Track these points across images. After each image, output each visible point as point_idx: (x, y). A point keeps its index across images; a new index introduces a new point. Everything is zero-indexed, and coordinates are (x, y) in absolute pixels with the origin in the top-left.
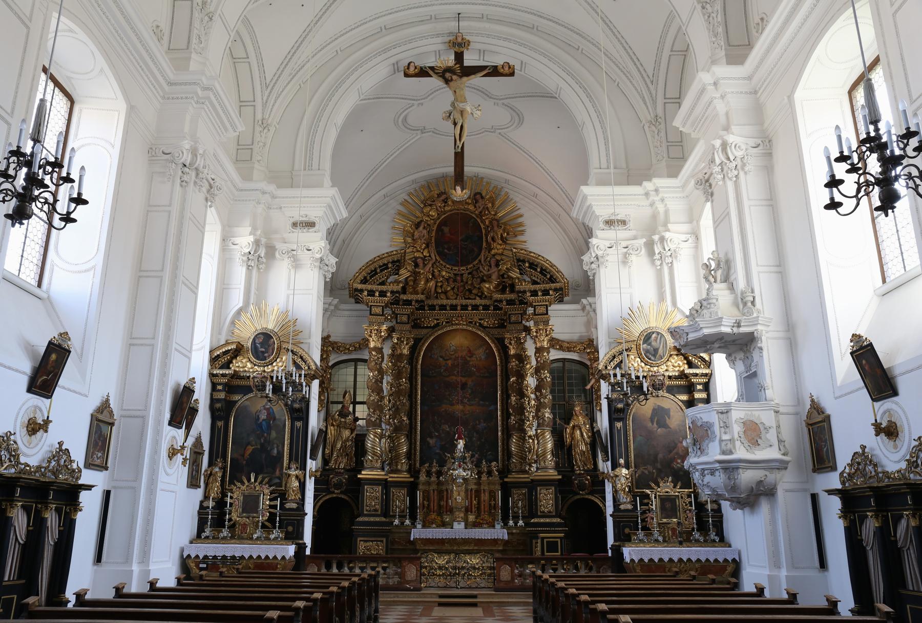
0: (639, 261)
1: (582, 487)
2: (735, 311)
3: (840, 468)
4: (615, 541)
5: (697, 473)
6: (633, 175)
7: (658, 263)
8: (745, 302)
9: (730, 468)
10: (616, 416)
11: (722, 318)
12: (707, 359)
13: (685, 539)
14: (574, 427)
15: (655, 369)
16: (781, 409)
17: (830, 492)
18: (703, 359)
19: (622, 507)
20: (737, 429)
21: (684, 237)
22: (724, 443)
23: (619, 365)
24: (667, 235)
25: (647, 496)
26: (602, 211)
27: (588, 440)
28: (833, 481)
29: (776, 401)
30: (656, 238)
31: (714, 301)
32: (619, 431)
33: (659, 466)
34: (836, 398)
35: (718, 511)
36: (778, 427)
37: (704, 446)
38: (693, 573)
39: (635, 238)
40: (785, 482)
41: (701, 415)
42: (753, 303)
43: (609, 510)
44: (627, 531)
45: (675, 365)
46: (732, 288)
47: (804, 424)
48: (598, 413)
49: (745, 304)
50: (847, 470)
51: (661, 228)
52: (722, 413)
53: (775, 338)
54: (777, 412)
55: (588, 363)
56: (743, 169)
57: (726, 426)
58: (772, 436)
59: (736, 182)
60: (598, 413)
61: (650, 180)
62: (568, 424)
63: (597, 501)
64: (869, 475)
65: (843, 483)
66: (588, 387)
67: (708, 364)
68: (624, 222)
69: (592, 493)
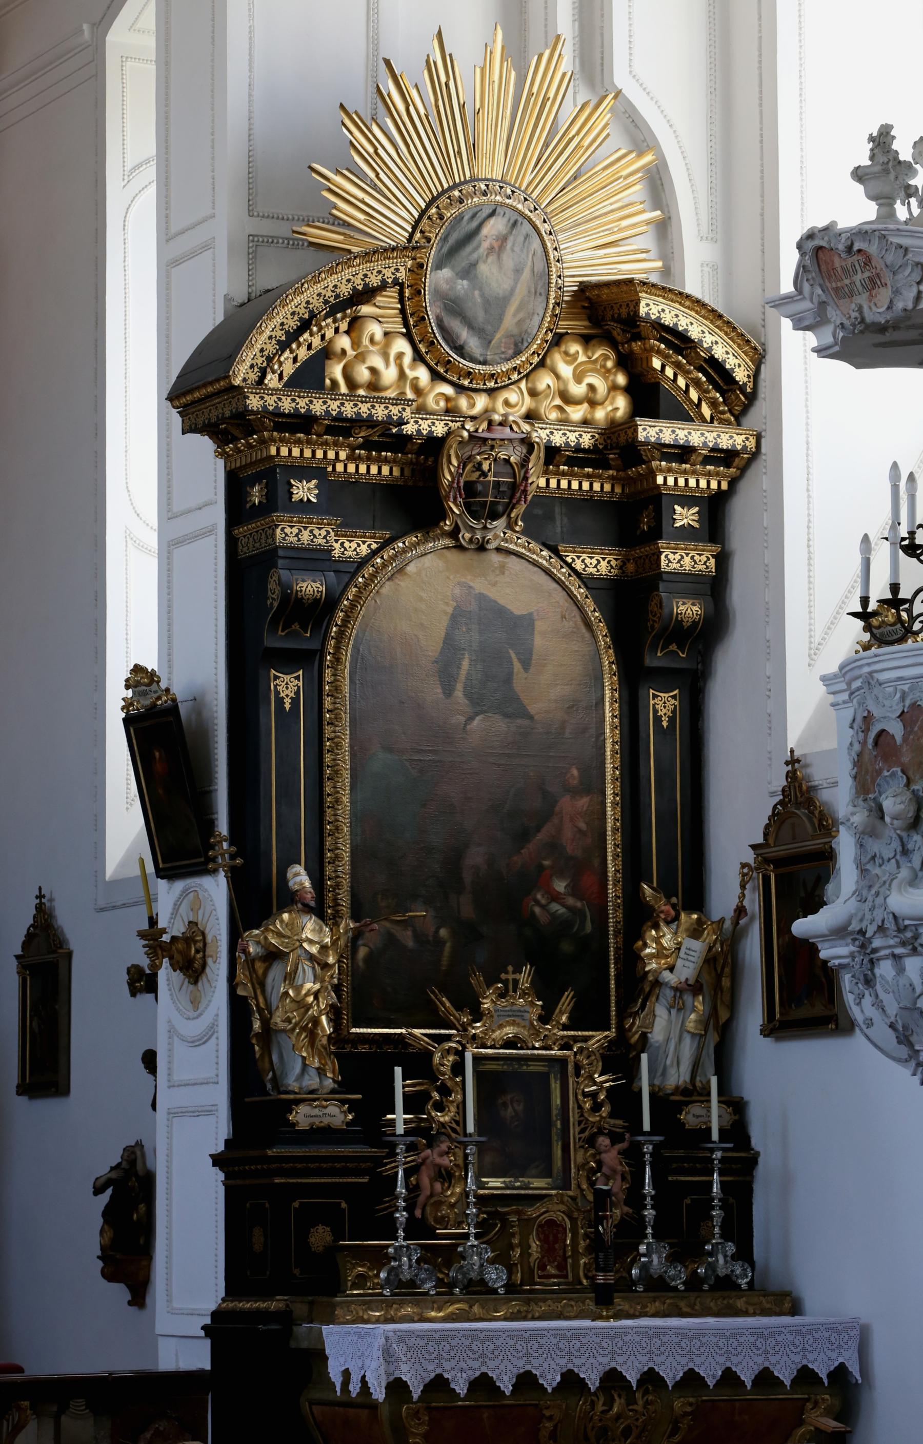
12: (741, 375)
15: (482, 402)
23: (311, 376)
32: (287, 719)
33: (466, 908)
44: (320, 1236)
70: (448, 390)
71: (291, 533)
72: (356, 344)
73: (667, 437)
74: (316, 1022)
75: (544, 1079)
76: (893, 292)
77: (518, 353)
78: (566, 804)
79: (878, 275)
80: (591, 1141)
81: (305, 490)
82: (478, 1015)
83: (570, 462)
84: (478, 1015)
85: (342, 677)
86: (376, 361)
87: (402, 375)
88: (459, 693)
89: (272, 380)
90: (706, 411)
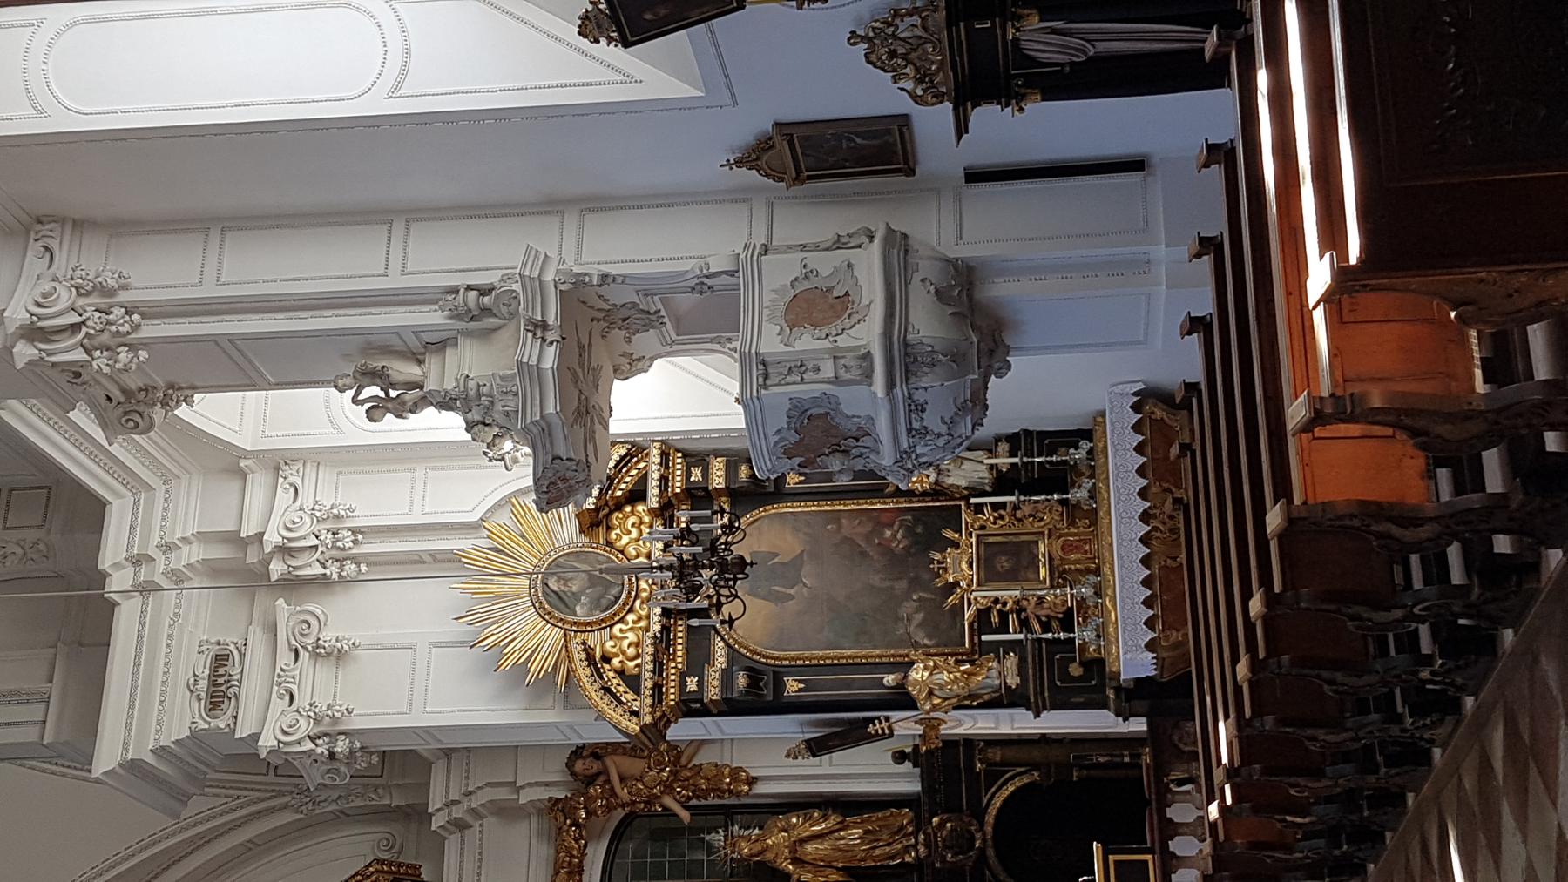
0: (338, 619)
1: (961, 841)
2: (505, 336)
3: (904, 105)
4: (1103, 705)
5: (919, 450)
6: (81, 626)
7: (350, 568)
8: (480, 311)
9: (905, 361)
10: (768, 694)
11: (520, 364)
12: (623, 451)
13: (1088, 516)
14: (796, 861)
16: (760, 239)
17: (962, 128)
18: (624, 461)
19: (1013, 681)
20: (806, 342)
21: (284, 497)
22: (842, 372)
23: (633, 682)
24: (272, 538)
25: (983, 615)
26: (180, 718)
27: (832, 821)
28: (933, 121)
29: (739, 250)
30: (277, 568)
31: (471, 384)
32: (809, 686)
33: (903, 584)
34: (736, 103)
35: (1015, 441)
36: (803, 248)
37: (850, 427)
38: (1175, 450)
39: (272, 630)
40: (938, 231)
41: (771, 432)
42: (484, 291)
43: (1018, 723)
44: (1075, 670)
45: (637, 535)
46: (440, 346)
47: (796, 190)
48: (761, 789)
49: (486, 311)
50: (909, 85)
51: (252, 558)
52: (766, 376)
53: (581, 228)
54: (766, 250)
55: (619, 814)
56: (111, 293)
57: (799, 367)
58: (824, 264)
59: (144, 316)
60: (761, 789)
61: (103, 577)
62: (788, 876)
63: (998, 801)
64: (919, 32)
65: (939, 98)
66: (685, 815)
67: (636, 450)
68: (221, 659)
69: (980, 815)
70: (638, 602)
71: (713, 692)
72: (617, 655)
73: (656, 491)
74: (964, 672)
75: (988, 545)
78: (846, 532)
80: (1019, 520)
81: (692, 683)
82: (956, 584)
84: (956, 584)
85: (786, 655)
86: (625, 643)
87: (631, 629)
88: (792, 591)
89: (636, 706)
90: (642, 465)
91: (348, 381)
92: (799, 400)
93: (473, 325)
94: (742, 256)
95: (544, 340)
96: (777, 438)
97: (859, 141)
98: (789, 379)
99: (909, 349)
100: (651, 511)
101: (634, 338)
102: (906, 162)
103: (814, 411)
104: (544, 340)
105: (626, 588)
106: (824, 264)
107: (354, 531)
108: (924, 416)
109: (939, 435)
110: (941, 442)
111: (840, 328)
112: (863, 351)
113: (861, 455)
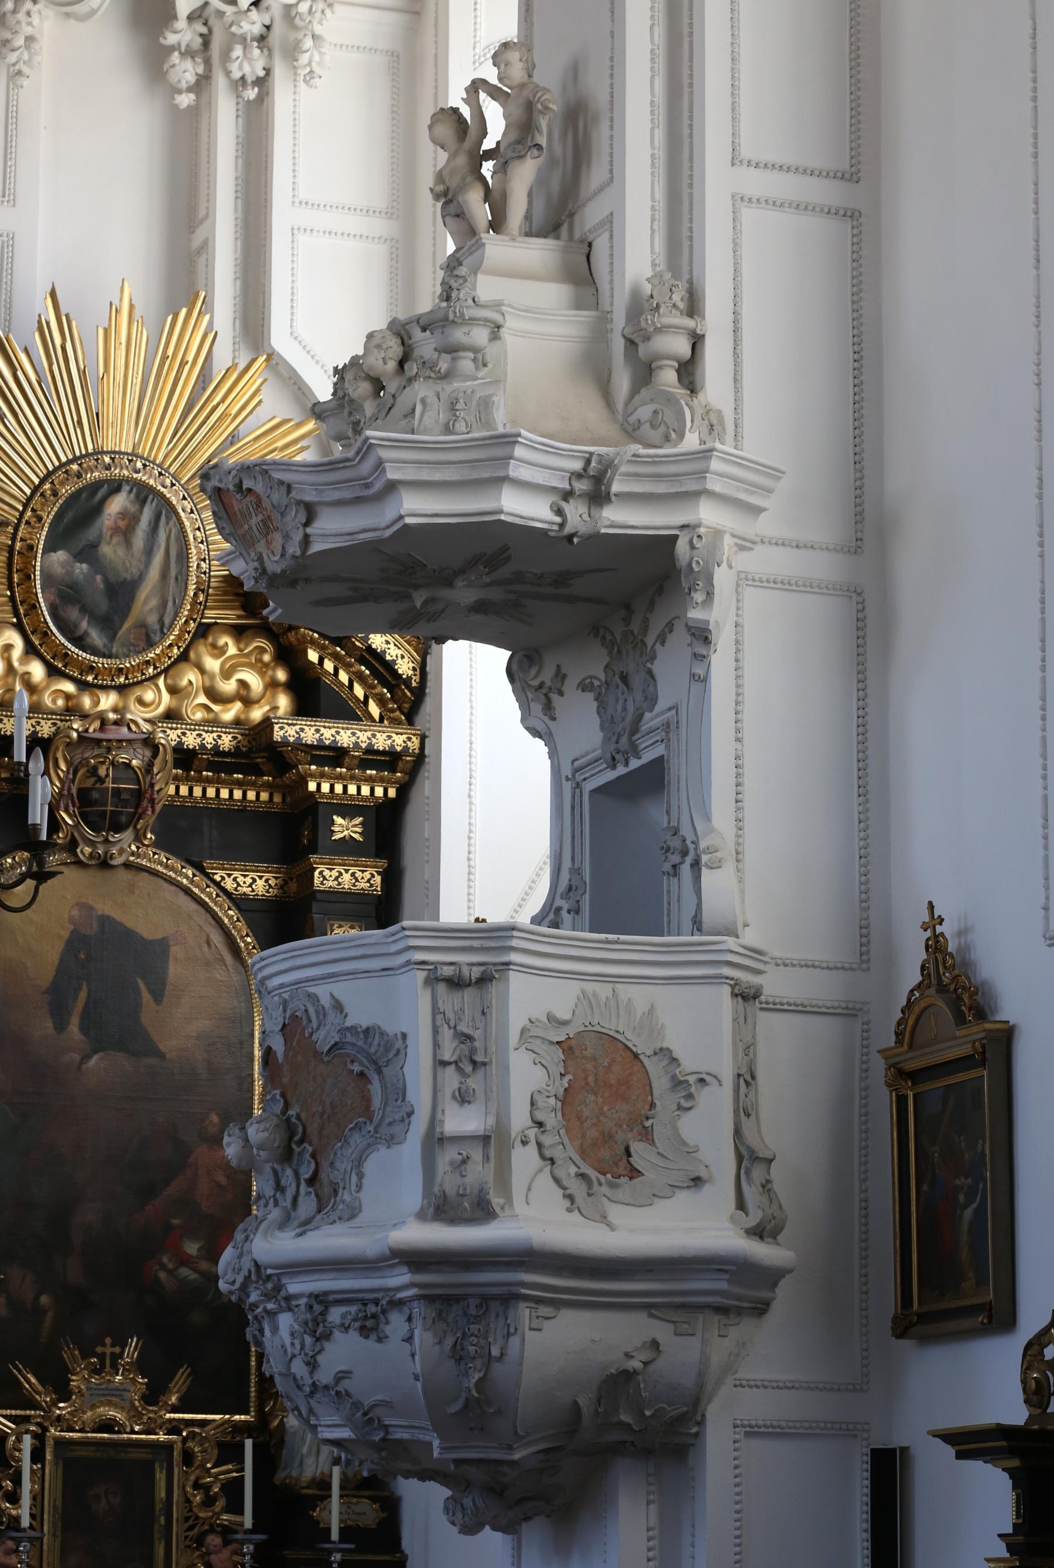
2: (589, 411)
5: (285, 1320)
7: (186, 71)
8: (643, 362)
9: (470, 1293)
11: (509, 440)
12: (405, 667)
15: (108, 701)
16: (774, 984)
17: (970, 1443)
18: (380, 668)
20: (527, 1078)
22: (448, 1156)
29: (750, 937)
31: (480, 336)
36: (746, 1079)
40: (753, 1386)
41: (342, 990)
42: (689, 371)
46: (582, 273)
47: (879, 1067)
49: (645, 372)
52: (456, 983)
54: (746, 996)
57: (470, 1060)
58: (707, 1128)
65: (1036, 1395)
70: (69, 687)
76: (284, 537)
77: (151, 644)
79: (269, 517)
80: (200, 1541)
83: (211, 766)
84: (64, 1393)
88: (74, 1027)
90: (374, 709)
91: (517, 72)
92: (401, 1053)
93: (618, 345)
94: (730, 942)
95: (567, 495)
96: (326, 1001)
97: (968, 1213)
98: (447, 1034)
99: (495, 1306)
100: (267, 724)
101: (590, 696)
102: (924, 1318)
103: (375, 1088)
104: (567, 495)
105: (101, 662)
106: (707, 1128)
107: (263, 82)
108: (354, 1335)
109: (312, 1365)
110: (299, 1368)
111: (558, 1153)
112: (496, 1201)
113: (279, 1188)
